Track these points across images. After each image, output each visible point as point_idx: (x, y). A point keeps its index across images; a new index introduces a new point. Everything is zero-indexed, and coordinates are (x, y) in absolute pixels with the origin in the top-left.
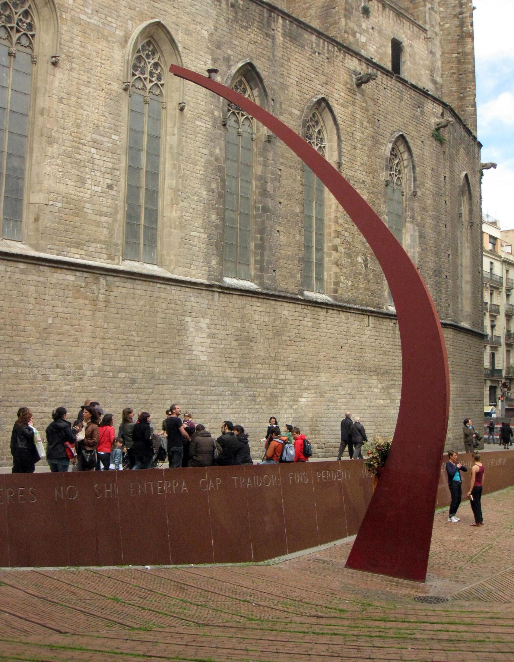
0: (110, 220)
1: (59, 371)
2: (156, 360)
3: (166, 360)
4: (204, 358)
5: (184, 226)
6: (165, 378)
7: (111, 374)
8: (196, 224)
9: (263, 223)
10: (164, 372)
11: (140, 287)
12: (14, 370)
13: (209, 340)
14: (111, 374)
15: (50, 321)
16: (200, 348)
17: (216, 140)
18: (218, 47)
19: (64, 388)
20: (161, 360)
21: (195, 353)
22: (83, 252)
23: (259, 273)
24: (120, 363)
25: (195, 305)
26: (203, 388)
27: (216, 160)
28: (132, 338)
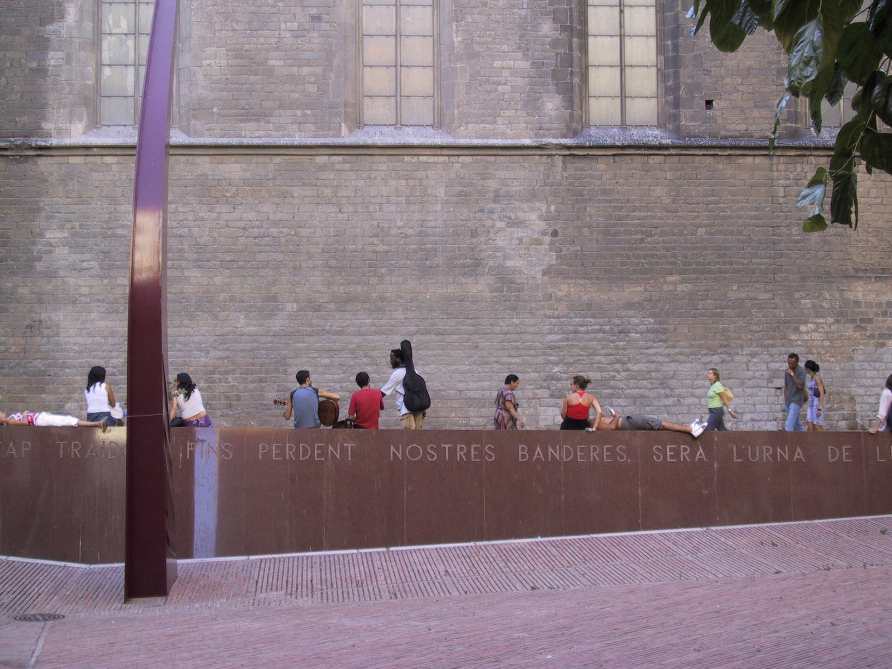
5: (476, 55)
9: (676, 18)
11: (383, 164)
23: (672, 111)
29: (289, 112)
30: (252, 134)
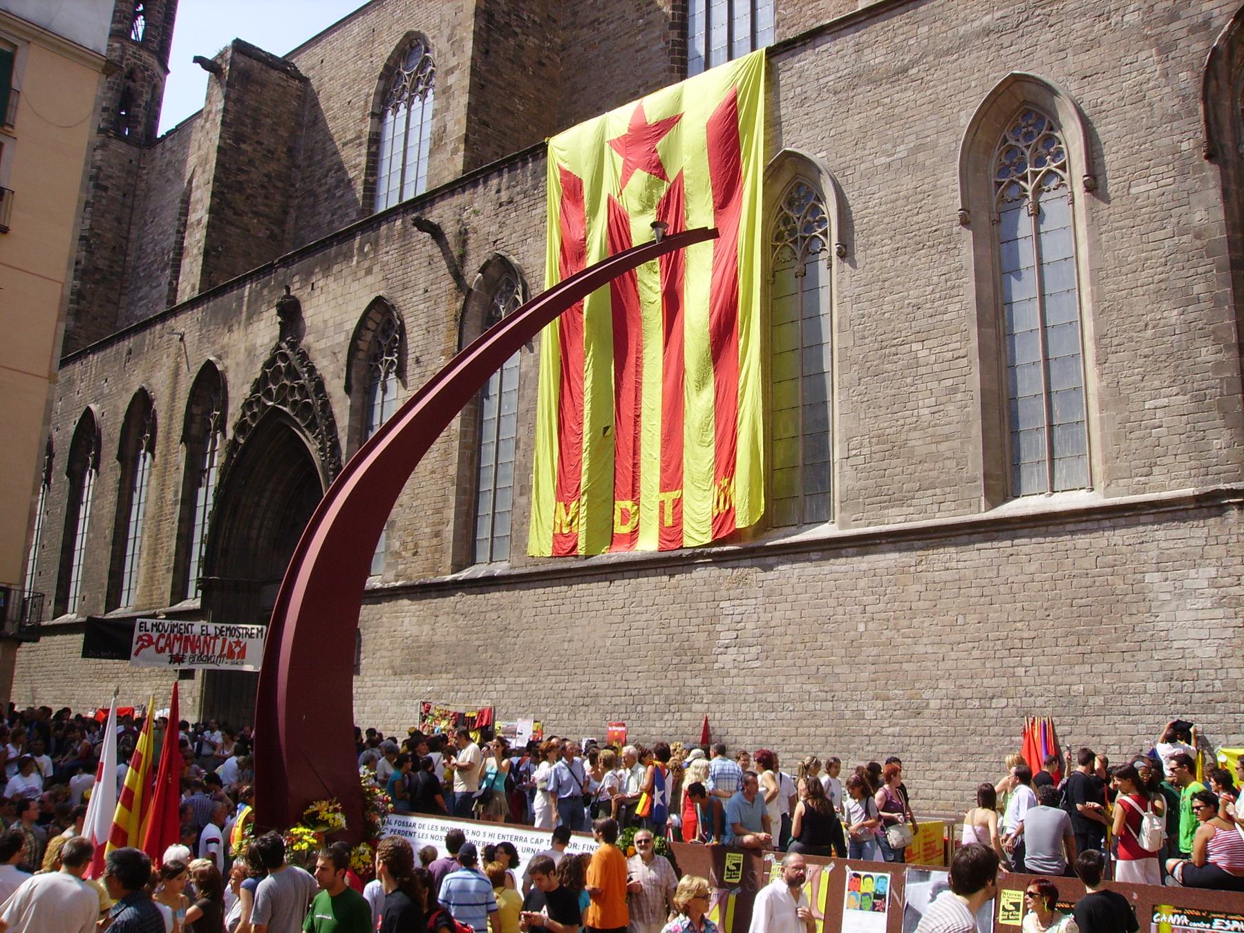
0: (957, 444)
1: (879, 704)
2: (1077, 669)
3: (1099, 668)
4: (1207, 651)
6: (1102, 703)
7: (977, 703)
8: (1157, 383)
10: (1096, 693)
12: (811, 706)
13: (1219, 613)
14: (977, 703)
15: (861, 627)
16: (1193, 633)
17: (1193, 198)
18: (1173, 16)
19: (891, 730)
20: (1087, 668)
21: (1176, 645)
22: (911, 510)
24: (994, 682)
25: (1170, 544)
26: (1211, 717)
27: (1198, 236)
28: (1017, 634)
29: (929, 492)
30: (895, 521)
